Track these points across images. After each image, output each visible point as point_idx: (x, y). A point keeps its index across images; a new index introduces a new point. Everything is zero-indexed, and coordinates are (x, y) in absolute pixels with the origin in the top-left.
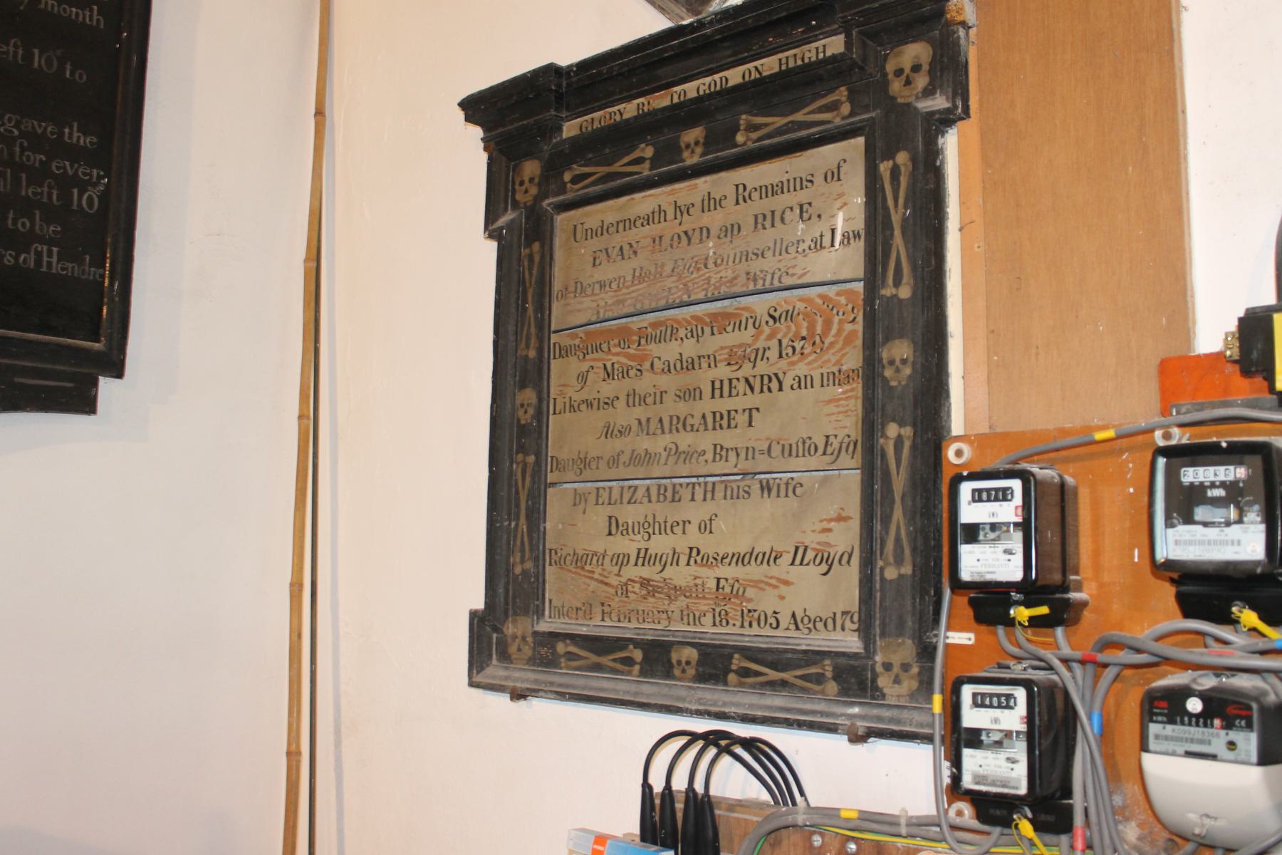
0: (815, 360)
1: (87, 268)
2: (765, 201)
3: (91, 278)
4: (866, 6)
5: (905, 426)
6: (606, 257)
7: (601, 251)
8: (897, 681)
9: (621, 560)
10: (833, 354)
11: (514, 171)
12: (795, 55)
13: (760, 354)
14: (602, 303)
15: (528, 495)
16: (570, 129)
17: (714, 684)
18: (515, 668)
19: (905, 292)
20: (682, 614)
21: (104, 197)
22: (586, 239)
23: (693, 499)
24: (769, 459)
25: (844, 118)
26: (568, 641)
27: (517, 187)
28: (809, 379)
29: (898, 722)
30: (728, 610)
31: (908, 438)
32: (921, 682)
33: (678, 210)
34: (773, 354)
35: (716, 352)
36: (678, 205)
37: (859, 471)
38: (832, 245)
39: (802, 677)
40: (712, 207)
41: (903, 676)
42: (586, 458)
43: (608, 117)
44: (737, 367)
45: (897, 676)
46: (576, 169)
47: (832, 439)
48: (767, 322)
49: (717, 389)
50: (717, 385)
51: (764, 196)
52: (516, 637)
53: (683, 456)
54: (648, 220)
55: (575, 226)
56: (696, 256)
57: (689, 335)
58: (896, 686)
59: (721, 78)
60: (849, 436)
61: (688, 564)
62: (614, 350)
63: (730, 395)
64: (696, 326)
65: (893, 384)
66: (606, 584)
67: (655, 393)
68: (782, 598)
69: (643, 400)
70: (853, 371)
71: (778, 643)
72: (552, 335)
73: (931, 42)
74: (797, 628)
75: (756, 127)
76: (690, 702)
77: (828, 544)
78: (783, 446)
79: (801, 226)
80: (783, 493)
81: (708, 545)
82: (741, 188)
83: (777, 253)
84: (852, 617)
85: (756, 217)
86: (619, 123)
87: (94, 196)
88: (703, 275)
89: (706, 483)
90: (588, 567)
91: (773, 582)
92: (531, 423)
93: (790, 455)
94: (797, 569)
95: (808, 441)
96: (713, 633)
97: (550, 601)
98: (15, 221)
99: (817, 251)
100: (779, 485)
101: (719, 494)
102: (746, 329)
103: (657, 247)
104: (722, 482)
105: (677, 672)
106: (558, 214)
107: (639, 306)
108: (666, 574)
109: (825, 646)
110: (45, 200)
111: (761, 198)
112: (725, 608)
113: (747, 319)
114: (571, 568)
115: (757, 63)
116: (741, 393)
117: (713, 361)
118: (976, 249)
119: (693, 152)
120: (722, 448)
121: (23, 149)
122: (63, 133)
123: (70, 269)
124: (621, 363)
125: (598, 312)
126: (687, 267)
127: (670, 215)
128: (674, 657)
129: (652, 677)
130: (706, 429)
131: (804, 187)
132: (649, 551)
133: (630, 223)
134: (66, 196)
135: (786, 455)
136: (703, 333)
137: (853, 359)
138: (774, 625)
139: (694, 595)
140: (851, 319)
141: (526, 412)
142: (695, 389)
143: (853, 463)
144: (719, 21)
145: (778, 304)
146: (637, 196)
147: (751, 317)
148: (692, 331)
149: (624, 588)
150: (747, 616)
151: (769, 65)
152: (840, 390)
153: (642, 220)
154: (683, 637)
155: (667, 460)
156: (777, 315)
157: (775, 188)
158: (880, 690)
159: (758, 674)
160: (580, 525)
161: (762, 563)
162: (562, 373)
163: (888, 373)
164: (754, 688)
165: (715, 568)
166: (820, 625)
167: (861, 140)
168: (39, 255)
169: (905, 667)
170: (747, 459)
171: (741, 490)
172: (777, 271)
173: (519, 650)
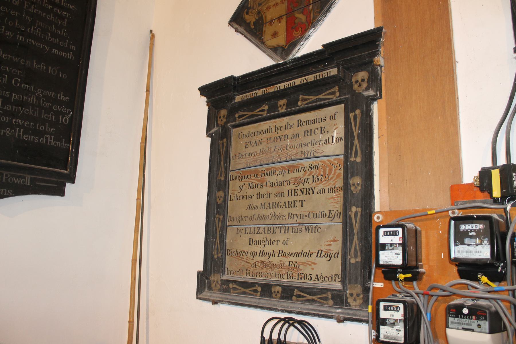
0: (326, 183)
1: (63, 144)
2: (308, 126)
3: (65, 147)
4: (345, 59)
5: (358, 208)
6: (250, 145)
7: (248, 142)
8: (355, 300)
9: (254, 254)
10: (332, 181)
11: (217, 113)
12: (320, 75)
13: (306, 181)
14: (249, 161)
15: (220, 230)
16: (238, 99)
17: (287, 300)
18: (214, 293)
19: (359, 160)
20: (276, 274)
21: (71, 119)
22: (243, 138)
23: (280, 233)
24: (309, 219)
25: (337, 97)
26: (234, 283)
27: (218, 119)
28: (323, 190)
29: (355, 315)
30: (293, 273)
31: (360, 212)
32: (363, 301)
33: (276, 128)
34: (310, 181)
35: (290, 179)
36: (277, 127)
37: (341, 224)
38: (332, 142)
39: (319, 298)
40: (289, 128)
41: (357, 298)
42: (241, 217)
43: (252, 95)
44: (297, 185)
45: (355, 298)
46: (240, 113)
47: (332, 212)
48: (308, 169)
49: (290, 193)
50: (290, 191)
51: (308, 124)
52: (215, 281)
53: (277, 217)
54: (266, 132)
55: (239, 133)
56: (283, 145)
57: (280, 173)
58: (355, 302)
59: (293, 82)
60: (338, 211)
61: (278, 256)
62: (253, 178)
63: (295, 195)
64: (283, 170)
65: (354, 192)
66: (248, 263)
67: (267, 194)
68: (313, 269)
69: (263, 196)
70: (340, 187)
71: (311, 286)
72: (230, 172)
73: (368, 71)
74: (318, 280)
75: (305, 100)
76: (279, 306)
77: (330, 250)
78: (314, 214)
79: (321, 135)
80: (313, 231)
81: (286, 249)
82: (299, 121)
83: (312, 145)
84: (338, 276)
85: (305, 132)
86: (256, 97)
87: (67, 118)
88: (285, 152)
89: (285, 227)
90: (241, 256)
91: (310, 263)
92: (222, 204)
93: (316, 217)
94: (318, 259)
95: (323, 212)
96: (287, 281)
97: (227, 268)
98: (39, 127)
99: (327, 144)
100: (312, 228)
101: (290, 231)
102: (301, 171)
103: (269, 141)
104: (292, 226)
105: (274, 295)
106: (233, 129)
107: (262, 162)
108: (270, 260)
109: (328, 287)
110: (50, 119)
111: (307, 125)
112: (292, 272)
113: (301, 168)
114: (235, 256)
115: (306, 77)
116: (299, 194)
117: (288, 183)
118: (384, 145)
119: (282, 108)
120: (291, 214)
123: (57, 145)
124: (255, 183)
125: (247, 164)
126: (280, 149)
127: (274, 130)
128: (273, 290)
129: (264, 297)
130: (286, 207)
131: (322, 121)
132: (264, 251)
133: (259, 133)
134: (57, 118)
135: (315, 217)
136: (285, 173)
137: (340, 183)
138: (310, 279)
139: (280, 267)
140: (339, 169)
141: (220, 200)
142: (282, 193)
143: (339, 221)
144: (293, 62)
145: (312, 163)
146: (262, 123)
147: (303, 167)
148: (281, 172)
149: (255, 264)
150: (300, 275)
151: (310, 78)
152: (335, 194)
153: (263, 132)
154: (276, 283)
155: (271, 218)
156: (312, 167)
157: (312, 122)
158: (349, 303)
159: (304, 297)
160: (239, 241)
161: (306, 256)
162: (233, 186)
163: (352, 188)
164: (302, 302)
165: (288, 258)
166: (327, 279)
167: (343, 105)
168: (47, 138)
169: (358, 295)
170: (300, 218)
171: (298, 230)
172: (312, 151)
173: (215, 286)
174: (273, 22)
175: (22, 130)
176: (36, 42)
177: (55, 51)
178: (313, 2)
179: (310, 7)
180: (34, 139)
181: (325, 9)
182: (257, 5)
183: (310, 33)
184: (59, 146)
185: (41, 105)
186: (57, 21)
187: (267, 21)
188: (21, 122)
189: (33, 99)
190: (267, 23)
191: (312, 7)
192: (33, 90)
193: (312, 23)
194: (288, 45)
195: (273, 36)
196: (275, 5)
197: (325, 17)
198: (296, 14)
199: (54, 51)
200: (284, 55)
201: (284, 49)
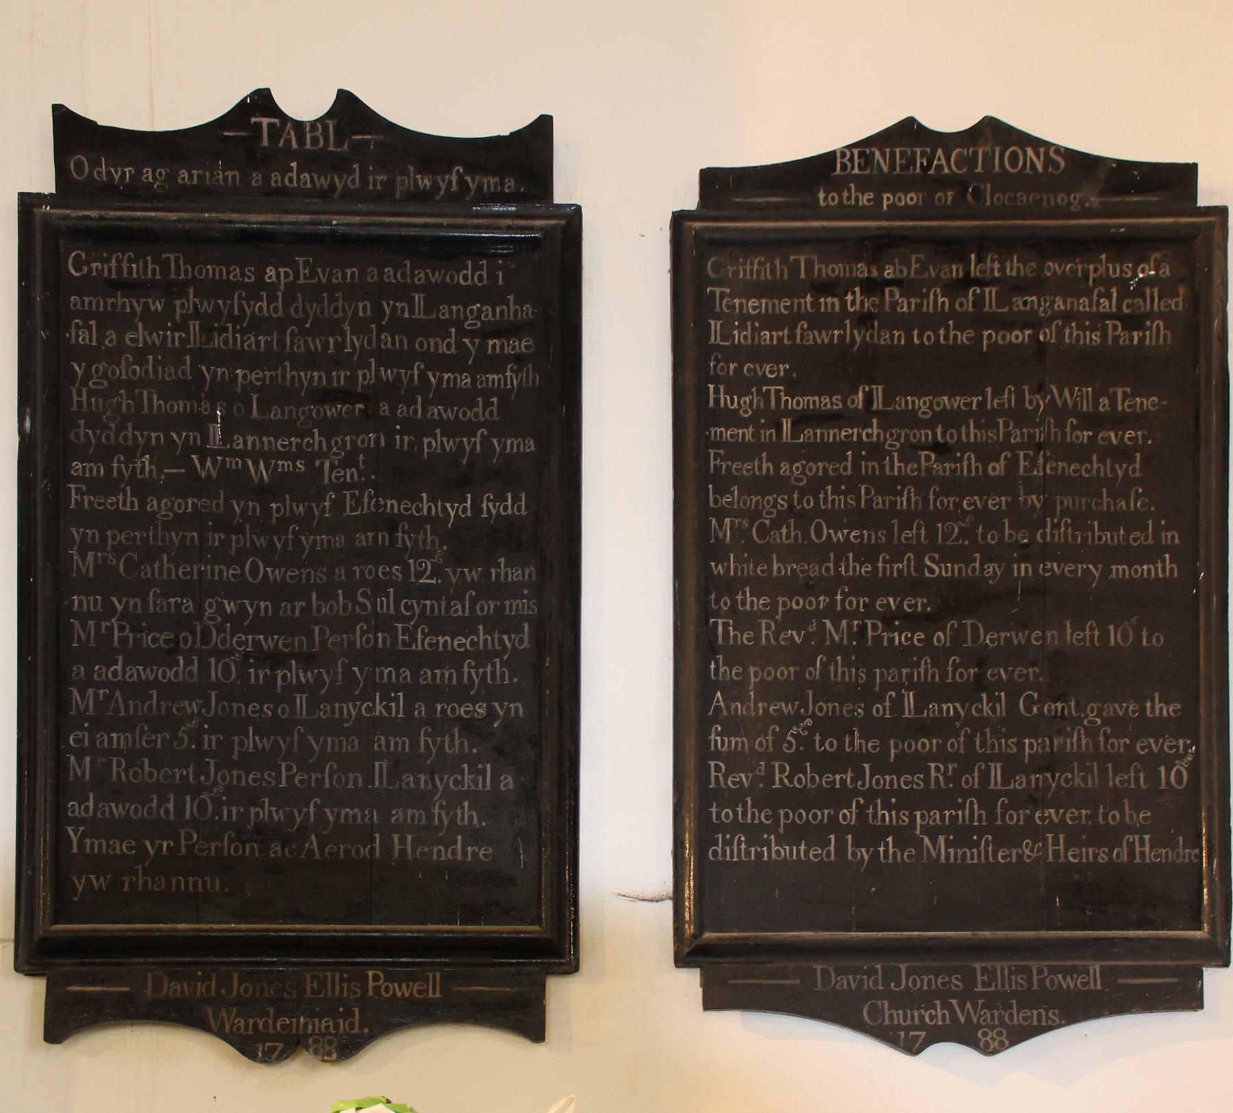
1: (1181, 851)
3: (1187, 861)
21: (1194, 769)
87: (1183, 770)
121: (1107, 737)
122: (1145, 708)
134: (1153, 777)
168: (1131, 846)
175: (1061, 836)
176: (1062, 565)
177: (1119, 570)
180: (1096, 856)
184: (1170, 860)
185: (1102, 749)
186: (1113, 470)
188: (1057, 813)
189: (1079, 740)
192: (1073, 713)
199: (1117, 570)
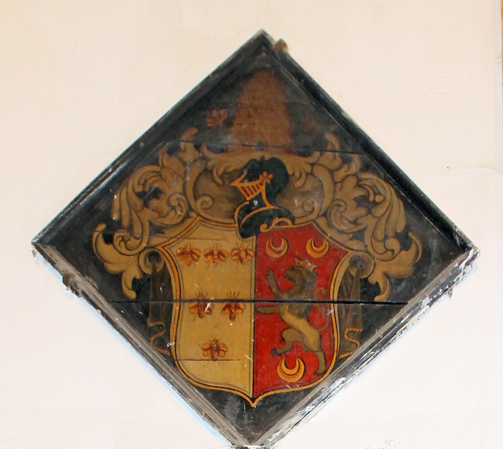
174: (209, 309)
178: (341, 300)
179: (332, 311)
181: (379, 333)
182: (147, 225)
183: (332, 387)
187: (187, 297)
190: (185, 301)
191: (336, 310)
193: (339, 361)
194: (261, 398)
195: (209, 352)
196: (211, 253)
197: (374, 357)
198: (286, 312)
200: (248, 425)
201: (249, 407)
